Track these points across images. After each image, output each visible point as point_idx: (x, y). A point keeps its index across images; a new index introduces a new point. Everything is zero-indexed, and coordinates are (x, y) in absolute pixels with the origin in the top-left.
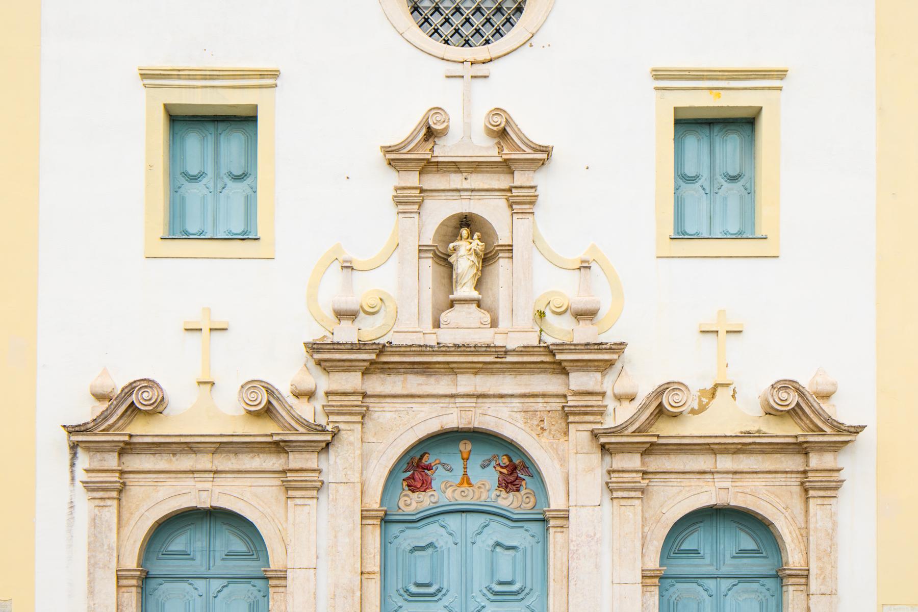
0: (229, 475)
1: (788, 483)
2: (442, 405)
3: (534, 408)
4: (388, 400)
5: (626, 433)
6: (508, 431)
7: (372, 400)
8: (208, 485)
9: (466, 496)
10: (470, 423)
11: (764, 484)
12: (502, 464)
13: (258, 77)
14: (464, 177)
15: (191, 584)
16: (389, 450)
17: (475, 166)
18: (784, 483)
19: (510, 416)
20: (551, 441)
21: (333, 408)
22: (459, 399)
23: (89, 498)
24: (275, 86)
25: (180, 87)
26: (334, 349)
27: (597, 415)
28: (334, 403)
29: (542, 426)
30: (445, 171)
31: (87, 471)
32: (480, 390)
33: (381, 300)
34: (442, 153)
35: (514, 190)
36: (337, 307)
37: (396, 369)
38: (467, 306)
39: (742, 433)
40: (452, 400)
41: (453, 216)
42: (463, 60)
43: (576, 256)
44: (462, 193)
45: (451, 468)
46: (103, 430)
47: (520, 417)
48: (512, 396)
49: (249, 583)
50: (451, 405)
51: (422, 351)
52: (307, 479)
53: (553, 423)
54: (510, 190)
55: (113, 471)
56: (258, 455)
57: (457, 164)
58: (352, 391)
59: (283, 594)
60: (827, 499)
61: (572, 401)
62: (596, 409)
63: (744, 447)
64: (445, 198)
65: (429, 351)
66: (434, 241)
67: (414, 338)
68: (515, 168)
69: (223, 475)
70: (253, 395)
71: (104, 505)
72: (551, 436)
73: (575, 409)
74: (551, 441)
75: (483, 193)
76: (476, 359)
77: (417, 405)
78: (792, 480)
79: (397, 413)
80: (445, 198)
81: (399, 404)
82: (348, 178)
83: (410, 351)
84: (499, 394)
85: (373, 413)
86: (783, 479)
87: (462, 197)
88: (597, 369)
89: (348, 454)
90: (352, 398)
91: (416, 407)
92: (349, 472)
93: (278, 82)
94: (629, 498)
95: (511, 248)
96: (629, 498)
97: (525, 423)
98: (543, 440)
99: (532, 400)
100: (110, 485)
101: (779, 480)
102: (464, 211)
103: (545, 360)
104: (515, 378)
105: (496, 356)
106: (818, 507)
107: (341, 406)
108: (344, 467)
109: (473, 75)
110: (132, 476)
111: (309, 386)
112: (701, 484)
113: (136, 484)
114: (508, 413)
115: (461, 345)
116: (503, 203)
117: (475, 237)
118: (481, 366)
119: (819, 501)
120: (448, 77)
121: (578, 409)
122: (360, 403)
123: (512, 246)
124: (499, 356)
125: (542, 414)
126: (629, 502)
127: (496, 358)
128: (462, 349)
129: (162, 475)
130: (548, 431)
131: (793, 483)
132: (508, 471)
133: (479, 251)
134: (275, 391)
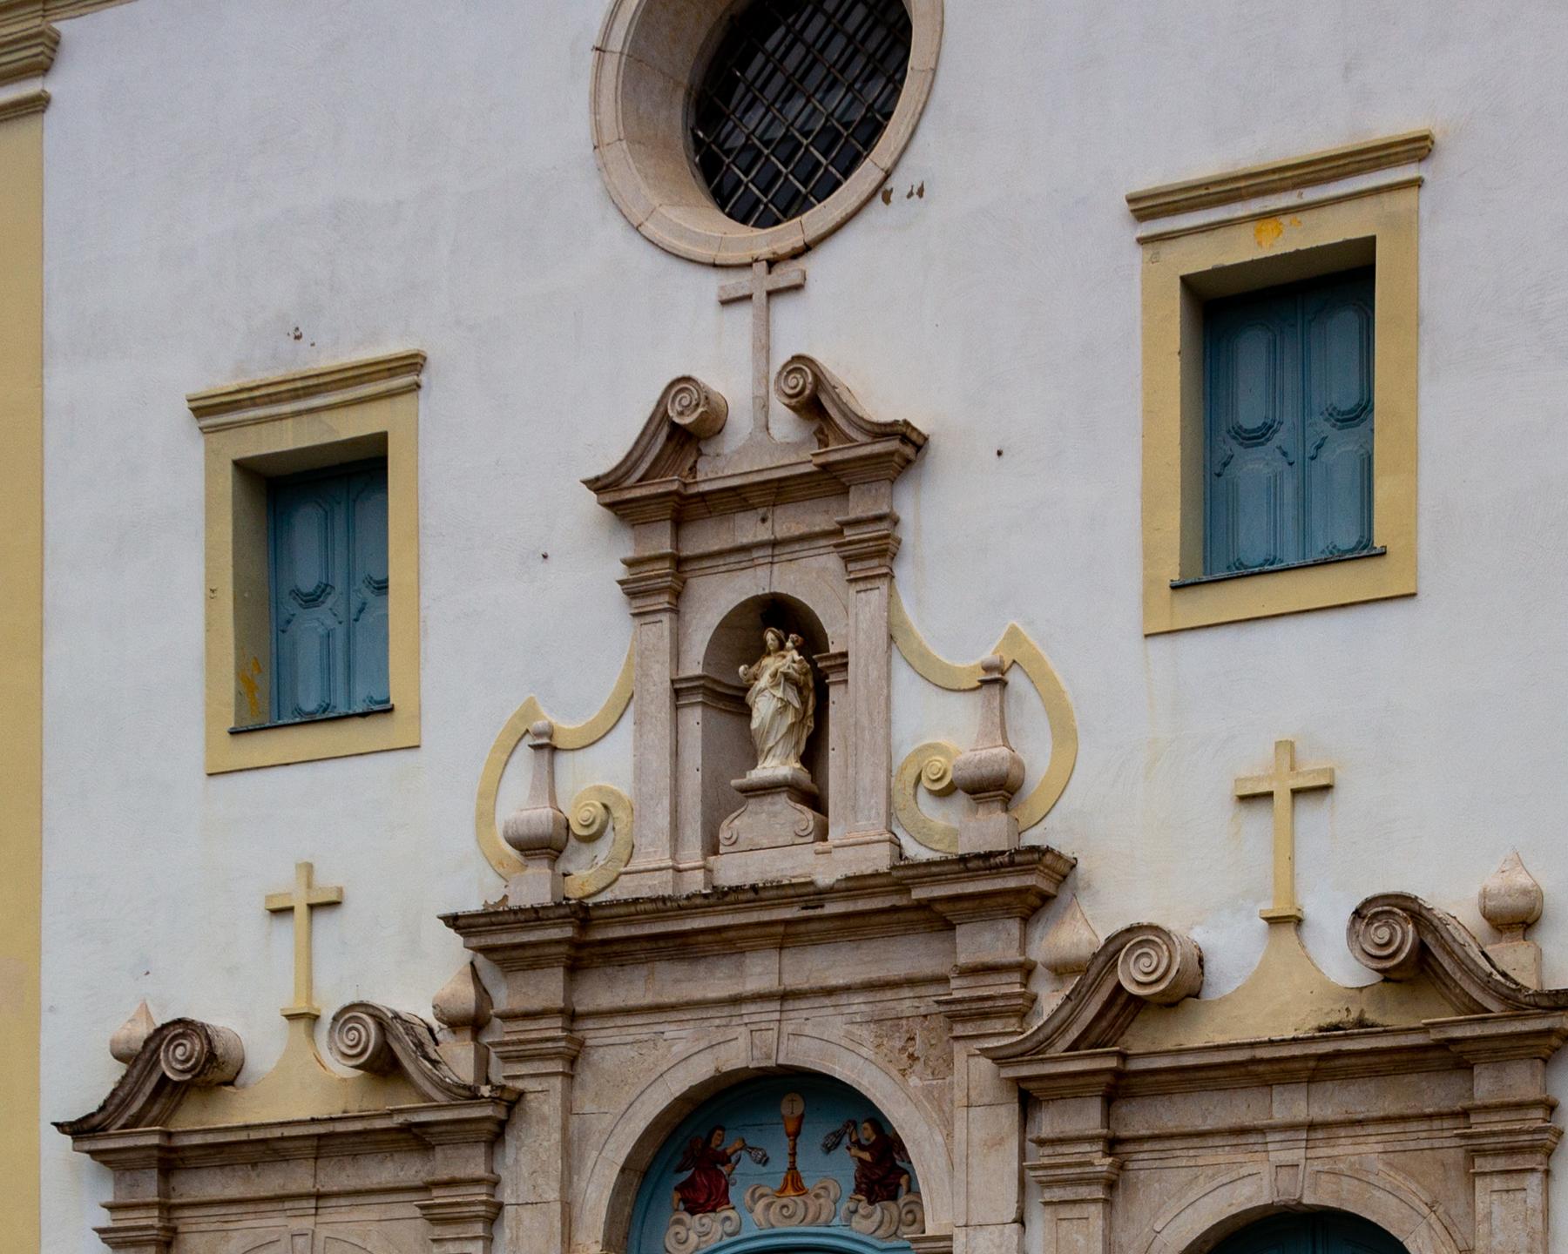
0: (343, 1202)
1: (1437, 1144)
2: (717, 1022)
4: (619, 1021)
6: (844, 1069)
7: (590, 1024)
8: (307, 1223)
9: (790, 1217)
10: (769, 1057)
11: (1380, 1148)
12: (863, 1142)
13: (386, 374)
14: (759, 518)
16: (619, 1127)
17: (775, 490)
18: (1425, 1144)
19: (849, 1035)
20: (928, 1082)
22: (748, 1006)
24: (415, 387)
25: (257, 421)
26: (493, 924)
27: (1009, 1017)
29: (911, 1050)
30: (722, 510)
31: (112, 1208)
33: (606, 807)
35: (846, 532)
37: (617, 954)
39: (1320, 1029)
40: (735, 1011)
43: (969, 660)
44: (755, 554)
45: (765, 1155)
47: (865, 1033)
48: (847, 989)
50: (736, 1021)
51: (658, 911)
52: (459, 1199)
53: (933, 1042)
54: (838, 532)
55: (147, 1206)
57: (739, 491)
60: (1515, 1176)
61: (959, 989)
62: (1001, 1003)
63: (1323, 1065)
64: (724, 568)
65: (672, 910)
66: (706, 664)
67: (656, 882)
68: (850, 481)
69: (333, 1202)
72: (929, 1071)
73: (959, 1007)
74: (928, 1082)
75: (797, 547)
76: (766, 916)
77: (673, 1027)
78: (1446, 1134)
79: (636, 1046)
80: (724, 568)
81: (638, 1029)
84: (822, 988)
85: (592, 1052)
86: (1424, 1135)
87: (756, 562)
88: (1008, 912)
89: (539, 1142)
90: (543, 1023)
91: (671, 1031)
92: (540, 1181)
93: (423, 379)
94: (1074, 1202)
96: (1074, 1202)
97: (878, 1046)
98: (914, 1081)
99: (889, 994)
100: (139, 1233)
101: (1415, 1136)
102: (760, 592)
103: (899, 903)
104: (858, 948)
105: (803, 905)
106: (1495, 1196)
107: (521, 1042)
110: (187, 1213)
111: (465, 1006)
112: (1240, 1158)
113: (194, 1228)
114: (844, 1027)
116: (832, 562)
117: (789, 644)
118: (781, 929)
119: (1498, 1183)
121: (966, 1006)
124: (810, 904)
125: (911, 1023)
126: (1075, 1212)
127: (803, 908)
130: (922, 1060)
131: (1447, 1143)
132: (871, 1154)
133: (796, 675)
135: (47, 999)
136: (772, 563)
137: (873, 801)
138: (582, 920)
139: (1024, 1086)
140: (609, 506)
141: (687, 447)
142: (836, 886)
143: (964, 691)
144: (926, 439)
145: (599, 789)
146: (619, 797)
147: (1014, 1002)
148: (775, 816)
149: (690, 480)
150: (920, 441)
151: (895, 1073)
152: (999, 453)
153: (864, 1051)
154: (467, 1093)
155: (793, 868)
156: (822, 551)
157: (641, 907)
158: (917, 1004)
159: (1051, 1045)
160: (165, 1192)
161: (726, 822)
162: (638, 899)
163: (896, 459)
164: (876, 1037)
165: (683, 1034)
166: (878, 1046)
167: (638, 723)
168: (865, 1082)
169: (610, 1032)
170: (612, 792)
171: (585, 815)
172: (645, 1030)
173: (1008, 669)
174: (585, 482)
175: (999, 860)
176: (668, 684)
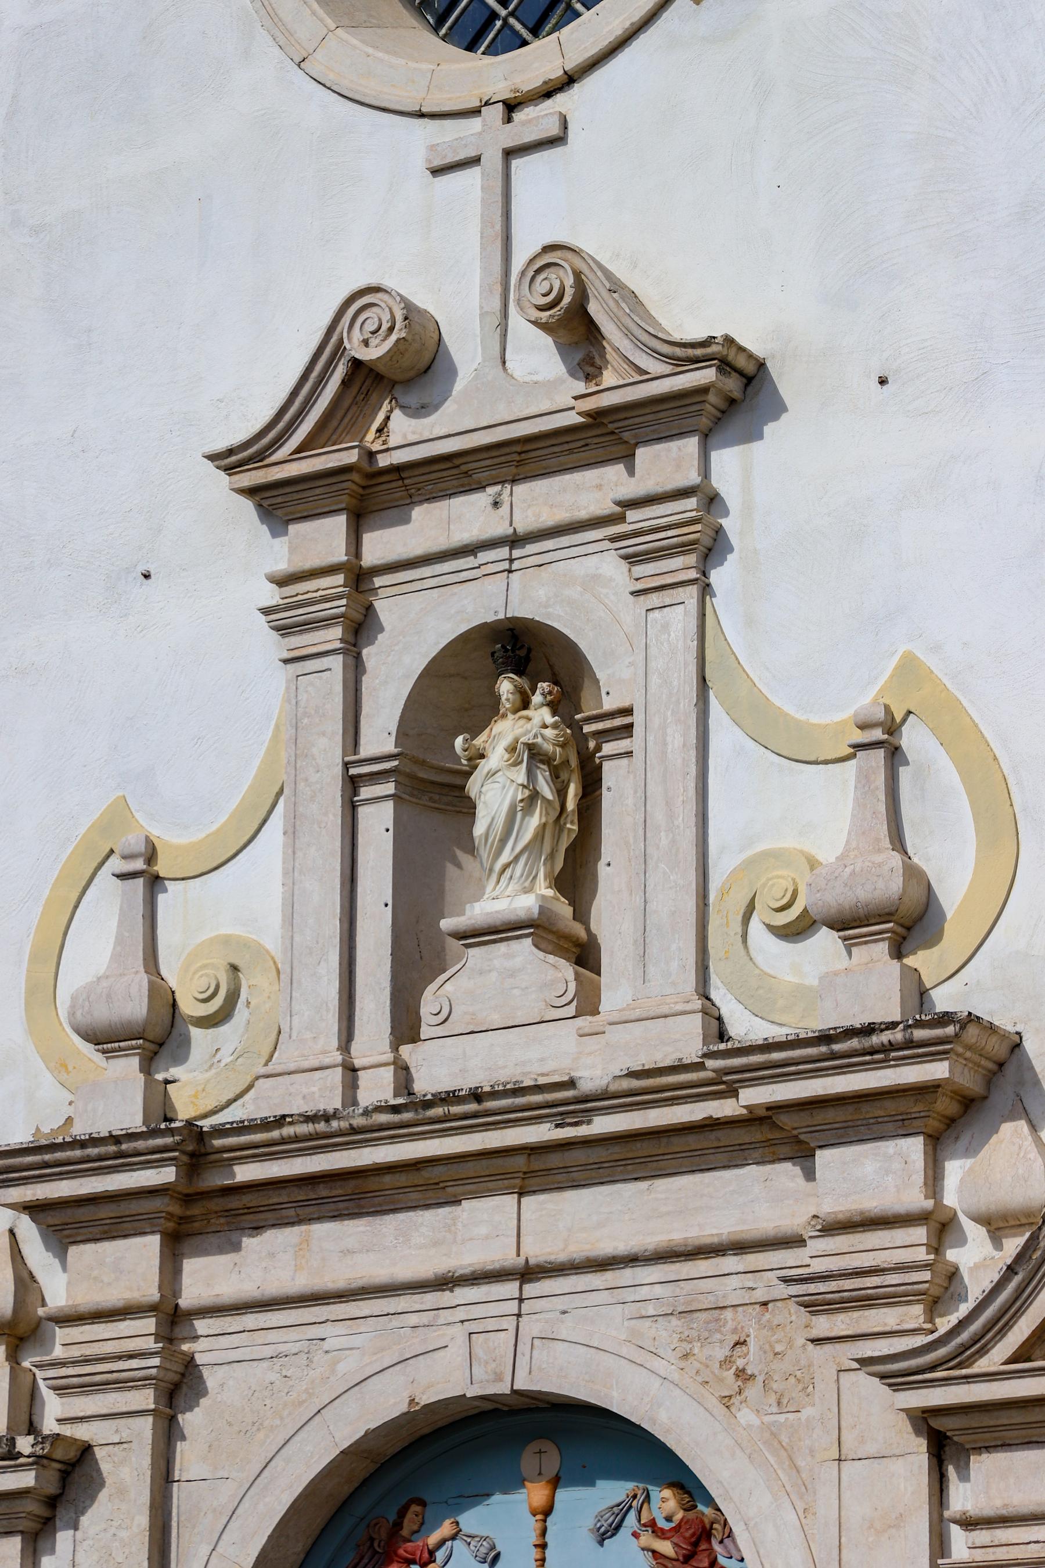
2: (413, 1320)
3: (710, 1297)
4: (251, 1320)
5: (982, 1365)
7: (202, 1326)
12: (662, 1523)
14: (491, 500)
16: (246, 1503)
20: (773, 1418)
29: (740, 1363)
32: (537, 1251)
34: (414, 433)
37: (250, 1210)
38: (502, 947)
41: (464, 640)
42: (478, 104)
45: (493, 1547)
48: (632, 1260)
53: (778, 1348)
67: (315, 1089)
72: (772, 1399)
73: (821, 1287)
74: (767, 1419)
77: (340, 1328)
82: (147, 576)
83: (283, 1141)
89: (113, 1530)
91: (336, 1336)
95: (626, 720)
97: (686, 1356)
98: (746, 1416)
102: (490, 618)
107: (87, 1361)
109: (510, 144)
115: (429, 1097)
117: (537, 699)
120: (437, 171)
123: (628, 711)
127: (557, 1126)
128: (438, 1111)
130: (760, 1379)
132: (676, 1545)
133: (549, 747)
136: (510, 571)
137: (674, 947)
138: (192, 1155)
139: (937, 1423)
140: (251, 492)
141: (374, 397)
142: (614, 1087)
143: (826, 762)
144: (761, 365)
145: (226, 941)
146: (259, 952)
147: (915, 1277)
148: (512, 976)
149: (376, 447)
150: (750, 368)
151: (713, 1403)
152: (883, 381)
153: (657, 1364)
155: (542, 1060)
156: (590, 548)
157: (288, 1131)
158: (751, 1284)
159: (983, 1351)
161: (431, 988)
162: (284, 1117)
163: (712, 398)
164: (681, 1340)
165: (357, 1341)
166: (686, 1356)
167: (292, 832)
168: (663, 1416)
169: (235, 1340)
170: (244, 944)
171: (201, 984)
172: (293, 1334)
173: (904, 720)
174: (212, 457)
175: (885, 1037)
176: (338, 770)
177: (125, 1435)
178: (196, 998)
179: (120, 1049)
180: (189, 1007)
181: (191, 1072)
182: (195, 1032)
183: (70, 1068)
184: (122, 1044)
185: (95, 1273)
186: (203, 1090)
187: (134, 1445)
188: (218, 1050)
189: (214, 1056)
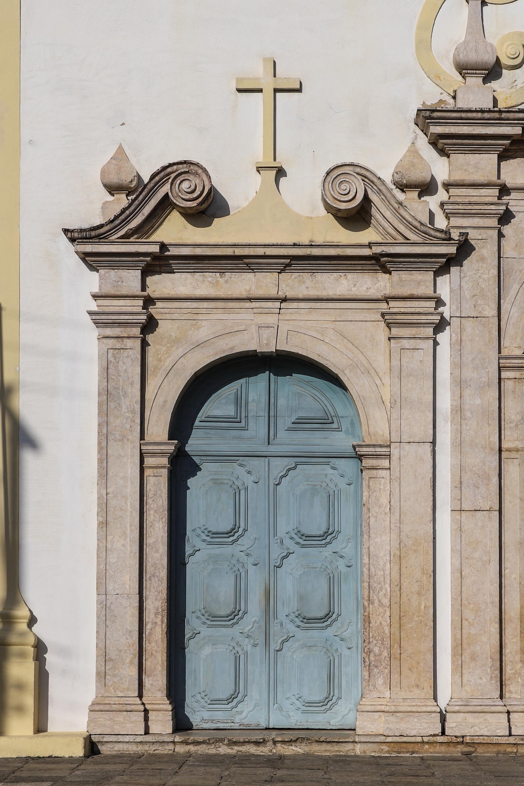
0: (302, 305)
8: (272, 319)
15: (241, 465)
21: (457, 207)
23: (99, 337)
28: (459, 200)
31: (95, 297)
36: (462, 58)
46: (122, 237)
49: (328, 464)
52: (421, 310)
55: (134, 297)
56: (345, 275)
58: (486, 182)
59: (383, 480)
70: (343, 187)
71: (122, 347)
90: (483, 192)
100: (131, 317)
107: (470, 204)
108: (473, 294)
113: (168, 316)
122: (495, 200)
129: (205, 304)
134: (375, 180)
135: (26, 134)
154: (443, 236)
160: (144, 287)
171: (511, 51)
177: (484, 236)
178: (509, 57)
179: (476, 74)
180: (505, 61)
181: (502, 88)
182: (504, 71)
183: (442, 79)
184: (477, 72)
185: (465, 168)
186: (510, 97)
187: (488, 241)
188: (516, 81)
189: (514, 83)
